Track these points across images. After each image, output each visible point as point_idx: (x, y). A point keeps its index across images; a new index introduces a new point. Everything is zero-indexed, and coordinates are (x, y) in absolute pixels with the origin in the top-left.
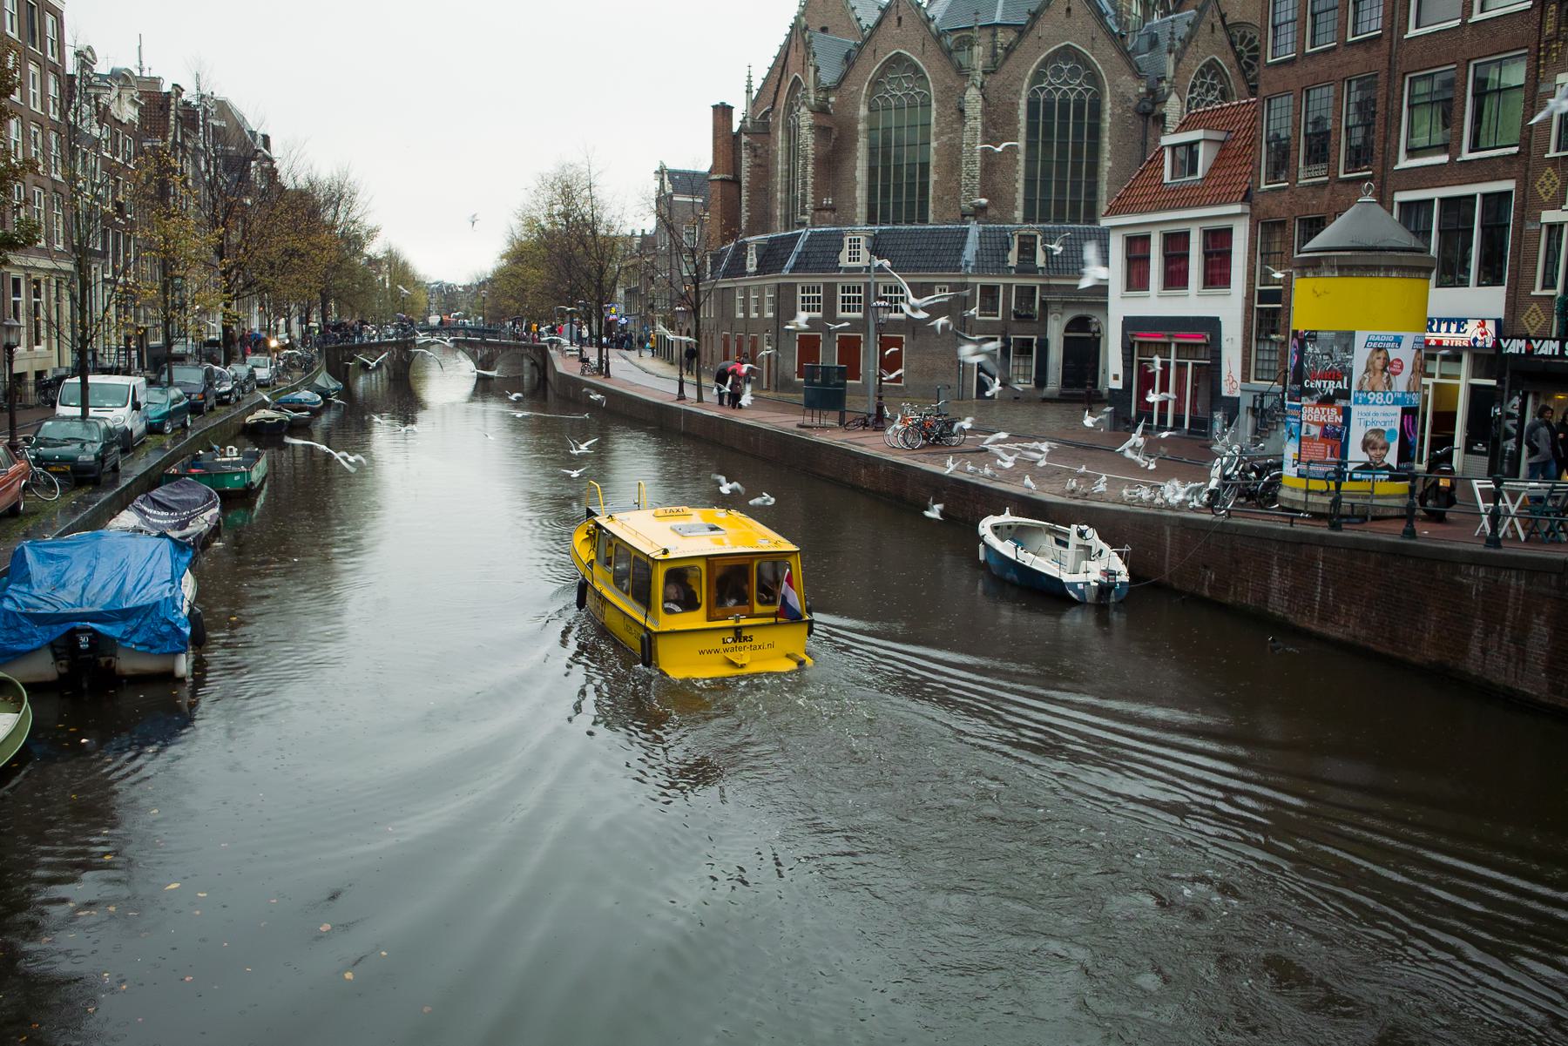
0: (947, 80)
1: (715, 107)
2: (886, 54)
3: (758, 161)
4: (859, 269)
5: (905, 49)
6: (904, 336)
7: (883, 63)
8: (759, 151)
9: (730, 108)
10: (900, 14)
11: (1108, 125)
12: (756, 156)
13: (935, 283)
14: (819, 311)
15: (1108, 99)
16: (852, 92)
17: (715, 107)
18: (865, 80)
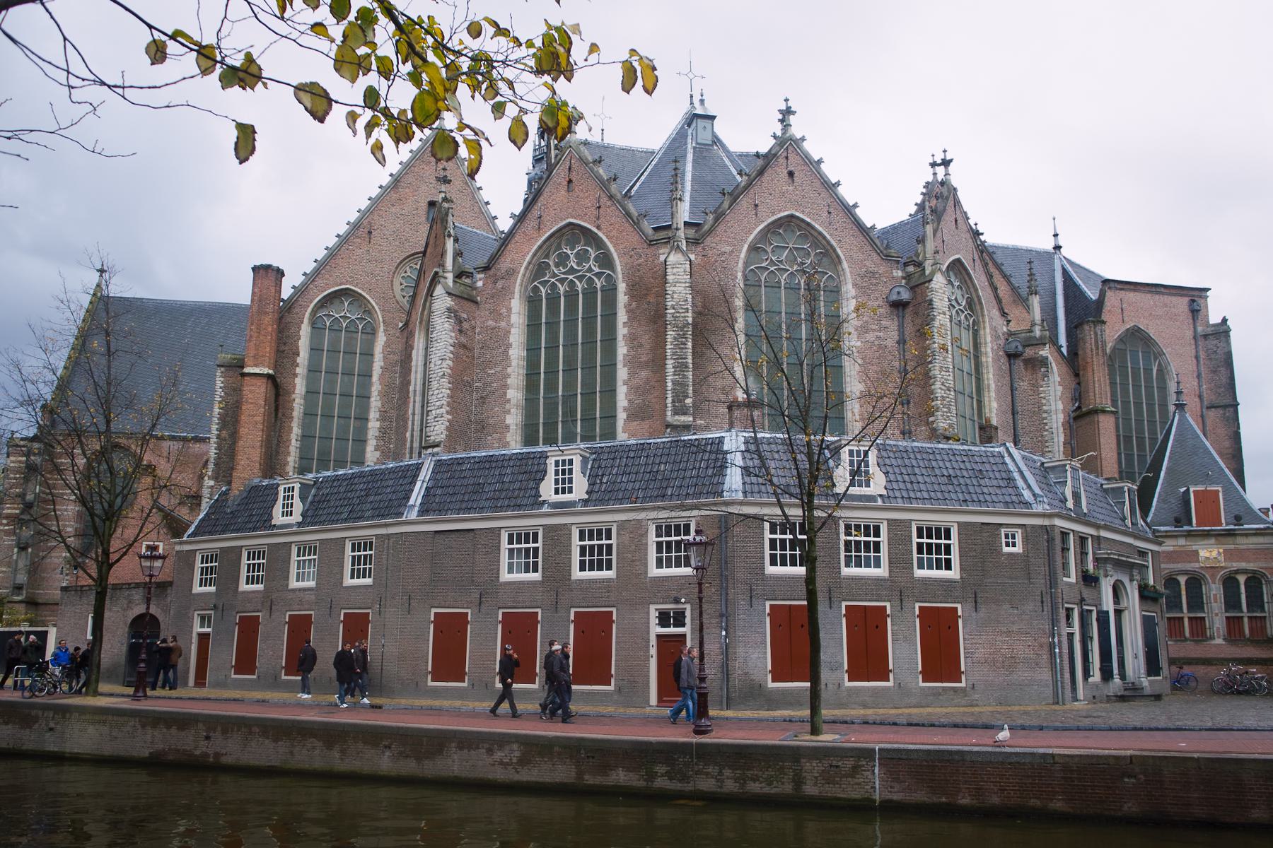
0: (868, 263)
1: (255, 269)
2: (773, 213)
3: (463, 340)
4: (871, 498)
5: (803, 212)
6: (959, 606)
7: (769, 225)
8: (466, 325)
9: (280, 273)
10: (791, 168)
11: (990, 360)
12: (460, 331)
13: (1001, 525)
14: (535, 570)
15: (988, 330)
16: (723, 254)
17: (255, 269)
18: (744, 240)
